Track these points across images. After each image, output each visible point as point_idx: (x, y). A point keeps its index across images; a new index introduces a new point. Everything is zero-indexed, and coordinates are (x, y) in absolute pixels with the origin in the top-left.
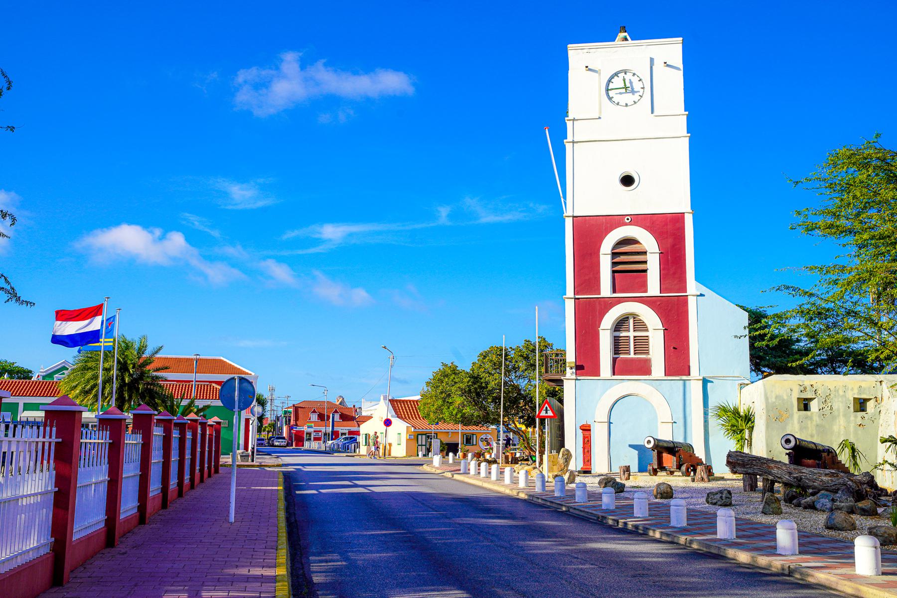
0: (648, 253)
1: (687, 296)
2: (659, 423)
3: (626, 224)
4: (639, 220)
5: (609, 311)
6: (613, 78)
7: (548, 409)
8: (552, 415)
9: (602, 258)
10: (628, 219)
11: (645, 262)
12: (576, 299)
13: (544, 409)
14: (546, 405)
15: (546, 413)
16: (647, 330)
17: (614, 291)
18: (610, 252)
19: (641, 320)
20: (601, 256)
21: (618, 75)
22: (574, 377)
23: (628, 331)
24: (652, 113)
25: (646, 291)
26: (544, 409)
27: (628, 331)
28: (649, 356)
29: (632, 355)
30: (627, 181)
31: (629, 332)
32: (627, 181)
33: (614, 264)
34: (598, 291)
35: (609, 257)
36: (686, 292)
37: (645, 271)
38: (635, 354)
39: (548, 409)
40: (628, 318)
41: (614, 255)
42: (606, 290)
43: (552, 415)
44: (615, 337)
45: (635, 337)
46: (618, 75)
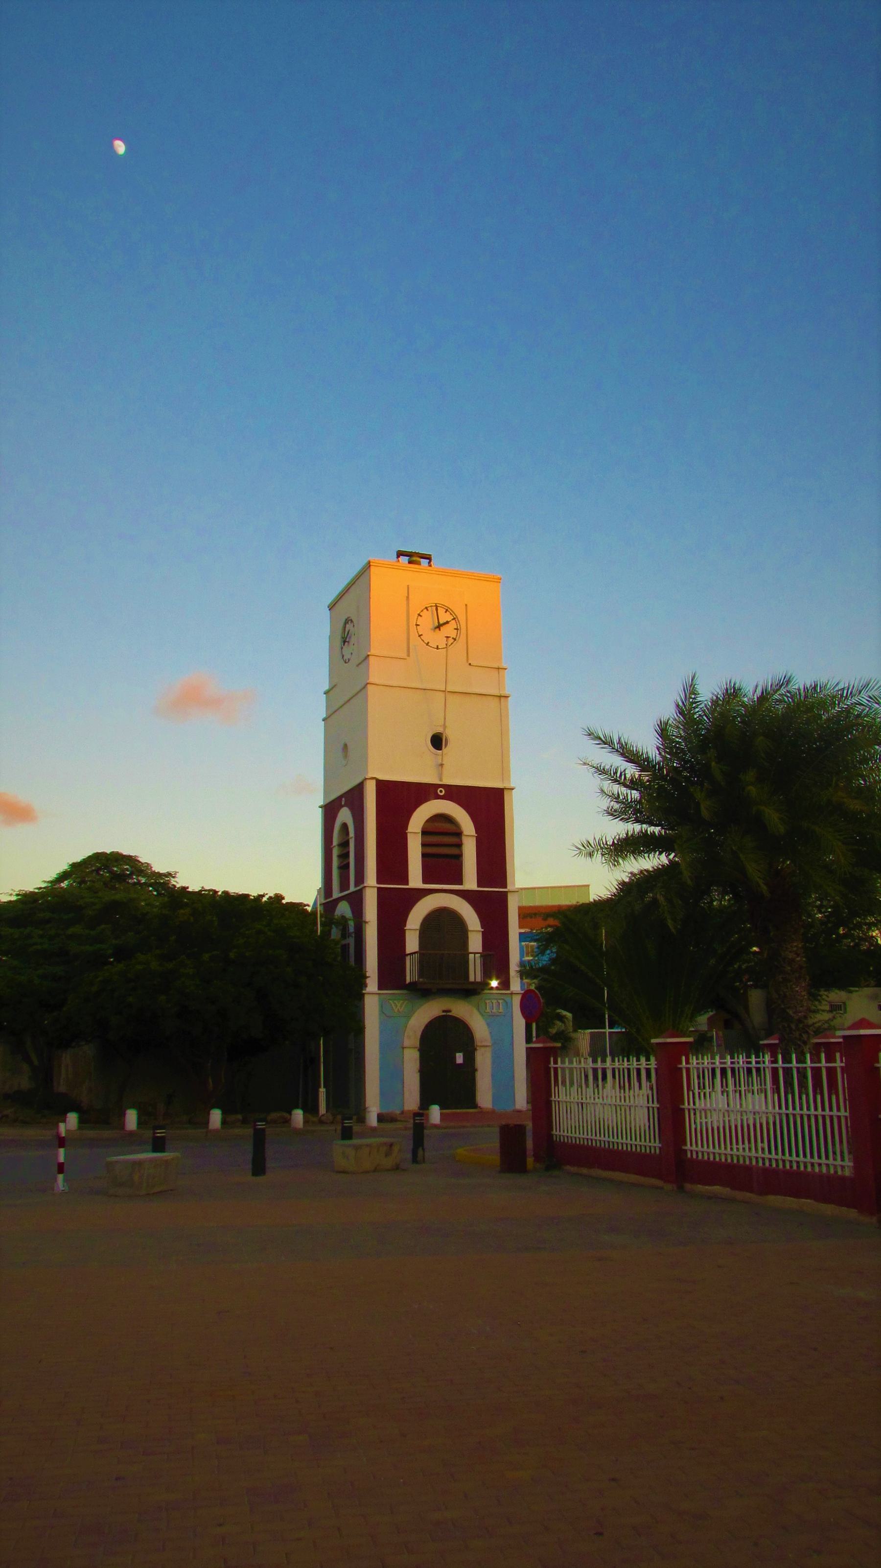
3: (438, 797)
4: (455, 793)
6: (422, 611)
10: (441, 791)
11: (459, 845)
17: (425, 881)
18: (419, 830)
20: (409, 836)
24: (467, 660)
30: (437, 741)
32: (437, 741)
33: (424, 845)
34: (404, 878)
36: (506, 887)
37: (459, 857)
41: (425, 832)
42: (415, 880)
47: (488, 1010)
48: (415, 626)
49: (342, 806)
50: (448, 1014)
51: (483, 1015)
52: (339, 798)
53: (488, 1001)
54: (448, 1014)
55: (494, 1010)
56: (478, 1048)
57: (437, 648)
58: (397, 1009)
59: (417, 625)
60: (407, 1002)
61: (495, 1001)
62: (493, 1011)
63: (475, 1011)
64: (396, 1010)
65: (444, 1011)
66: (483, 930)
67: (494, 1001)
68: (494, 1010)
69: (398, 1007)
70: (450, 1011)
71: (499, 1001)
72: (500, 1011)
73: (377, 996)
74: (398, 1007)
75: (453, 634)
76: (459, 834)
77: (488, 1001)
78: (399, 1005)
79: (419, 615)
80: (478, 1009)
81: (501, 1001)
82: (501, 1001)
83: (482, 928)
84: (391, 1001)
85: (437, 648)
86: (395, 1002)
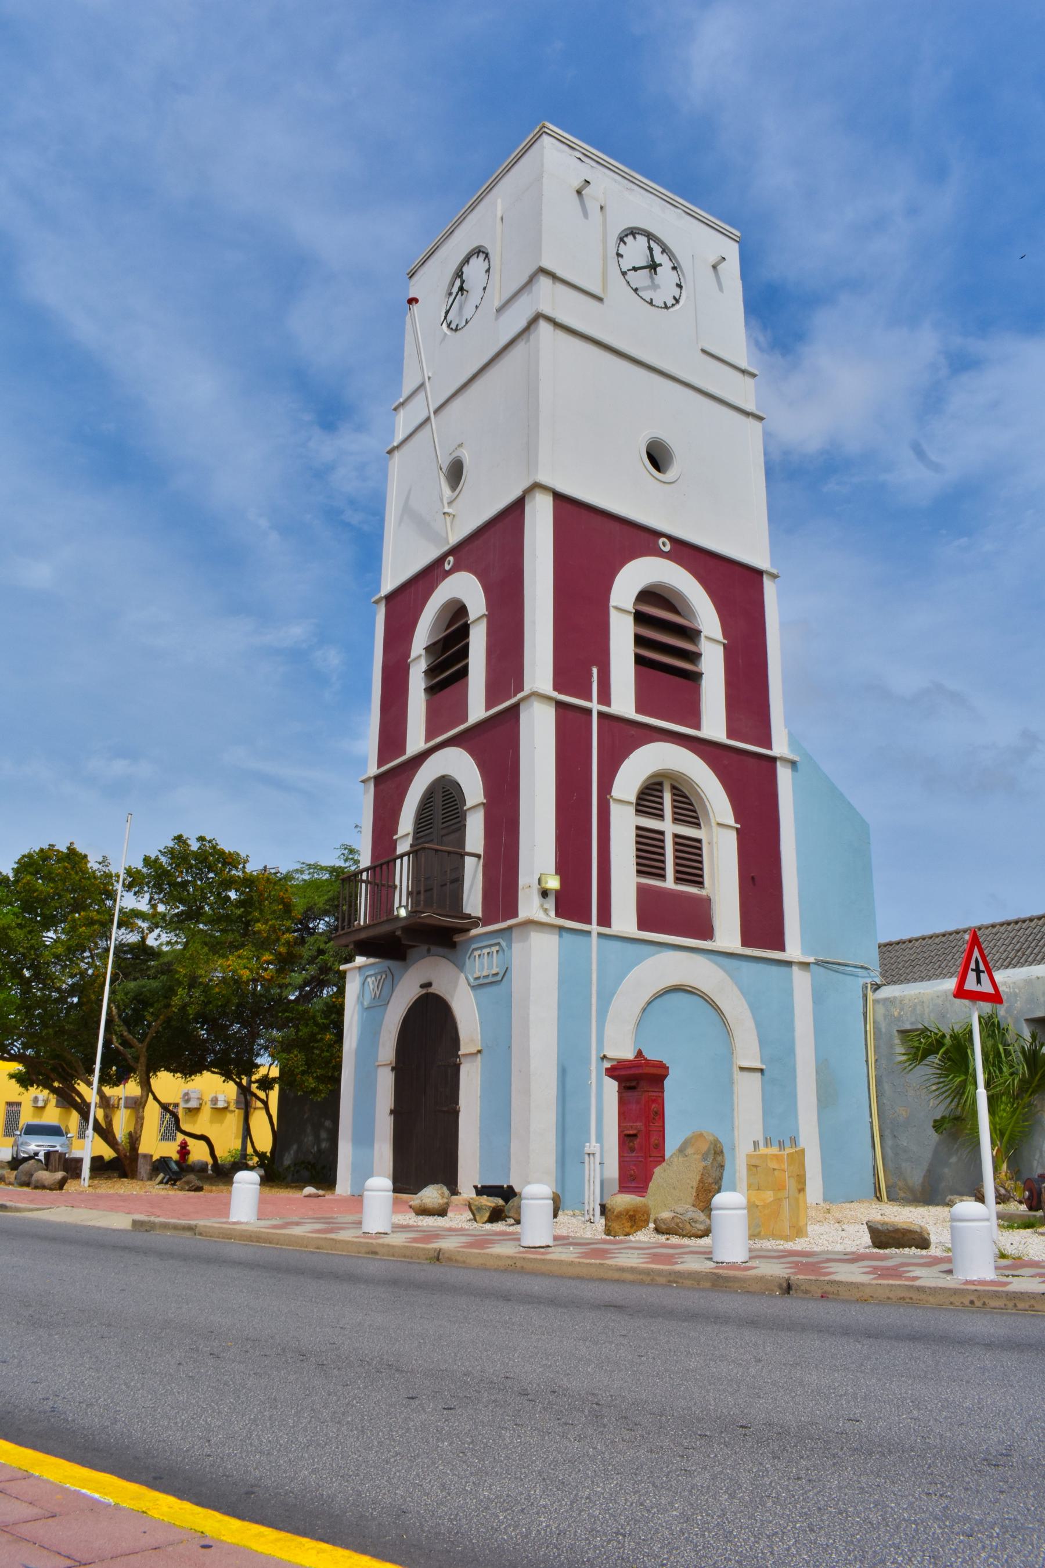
0: (703, 639)
1: (773, 760)
2: (736, 1070)
5: (631, 756)
6: (626, 236)
7: (982, 967)
8: (994, 992)
9: (615, 617)
10: (664, 544)
11: (694, 657)
12: (560, 705)
13: (973, 965)
14: (976, 953)
15: (979, 981)
16: (698, 825)
19: (686, 797)
21: (637, 236)
22: (552, 918)
23: (661, 817)
25: (698, 727)
26: (973, 965)
27: (661, 817)
28: (704, 893)
29: (669, 883)
31: (663, 820)
35: (630, 619)
37: (694, 678)
38: (678, 880)
39: (982, 967)
40: (661, 784)
41: (640, 618)
43: (994, 992)
44: (638, 828)
45: (676, 836)
46: (637, 236)
48: (616, 257)
49: (448, 573)
52: (440, 561)
57: (651, 303)
59: (619, 255)
66: (739, 826)
73: (557, 931)
75: (676, 292)
76: (692, 634)
79: (622, 240)
83: (736, 822)
85: (651, 303)
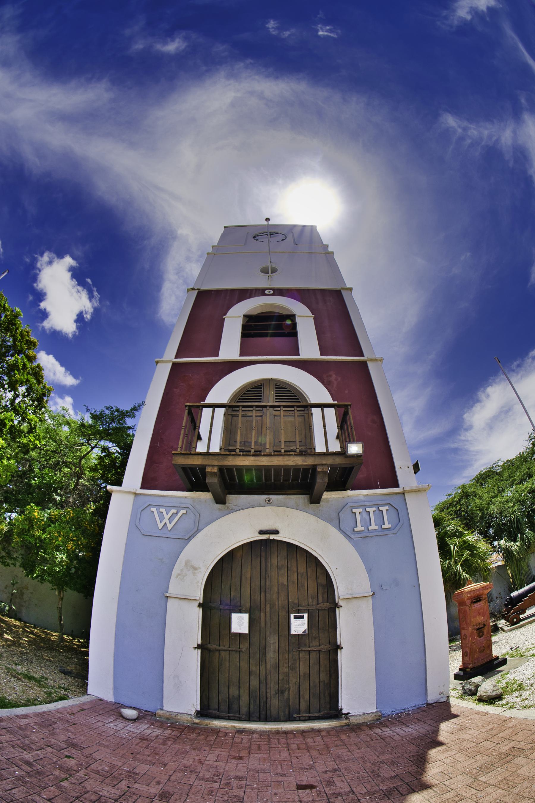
47: (359, 528)
50: (272, 537)
51: (348, 537)
53: (357, 511)
54: (272, 537)
55: (373, 527)
56: (341, 603)
58: (163, 523)
60: (183, 512)
61: (374, 509)
62: (370, 528)
63: (333, 531)
64: (160, 526)
65: (261, 532)
67: (371, 510)
68: (373, 527)
69: (166, 520)
70: (276, 532)
71: (381, 508)
72: (386, 525)
74: (166, 520)
77: (357, 511)
78: (167, 517)
80: (340, 529)
81: (384, 509)
82: (384, 509)
84: (152, 509)
86: (161, 510)
